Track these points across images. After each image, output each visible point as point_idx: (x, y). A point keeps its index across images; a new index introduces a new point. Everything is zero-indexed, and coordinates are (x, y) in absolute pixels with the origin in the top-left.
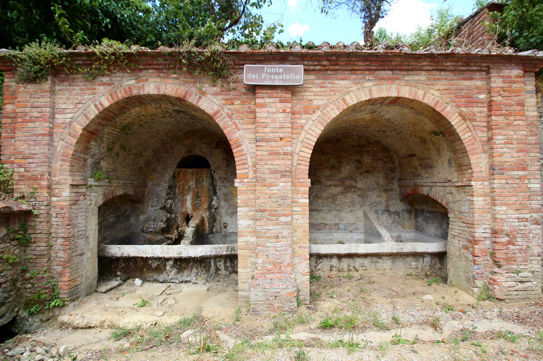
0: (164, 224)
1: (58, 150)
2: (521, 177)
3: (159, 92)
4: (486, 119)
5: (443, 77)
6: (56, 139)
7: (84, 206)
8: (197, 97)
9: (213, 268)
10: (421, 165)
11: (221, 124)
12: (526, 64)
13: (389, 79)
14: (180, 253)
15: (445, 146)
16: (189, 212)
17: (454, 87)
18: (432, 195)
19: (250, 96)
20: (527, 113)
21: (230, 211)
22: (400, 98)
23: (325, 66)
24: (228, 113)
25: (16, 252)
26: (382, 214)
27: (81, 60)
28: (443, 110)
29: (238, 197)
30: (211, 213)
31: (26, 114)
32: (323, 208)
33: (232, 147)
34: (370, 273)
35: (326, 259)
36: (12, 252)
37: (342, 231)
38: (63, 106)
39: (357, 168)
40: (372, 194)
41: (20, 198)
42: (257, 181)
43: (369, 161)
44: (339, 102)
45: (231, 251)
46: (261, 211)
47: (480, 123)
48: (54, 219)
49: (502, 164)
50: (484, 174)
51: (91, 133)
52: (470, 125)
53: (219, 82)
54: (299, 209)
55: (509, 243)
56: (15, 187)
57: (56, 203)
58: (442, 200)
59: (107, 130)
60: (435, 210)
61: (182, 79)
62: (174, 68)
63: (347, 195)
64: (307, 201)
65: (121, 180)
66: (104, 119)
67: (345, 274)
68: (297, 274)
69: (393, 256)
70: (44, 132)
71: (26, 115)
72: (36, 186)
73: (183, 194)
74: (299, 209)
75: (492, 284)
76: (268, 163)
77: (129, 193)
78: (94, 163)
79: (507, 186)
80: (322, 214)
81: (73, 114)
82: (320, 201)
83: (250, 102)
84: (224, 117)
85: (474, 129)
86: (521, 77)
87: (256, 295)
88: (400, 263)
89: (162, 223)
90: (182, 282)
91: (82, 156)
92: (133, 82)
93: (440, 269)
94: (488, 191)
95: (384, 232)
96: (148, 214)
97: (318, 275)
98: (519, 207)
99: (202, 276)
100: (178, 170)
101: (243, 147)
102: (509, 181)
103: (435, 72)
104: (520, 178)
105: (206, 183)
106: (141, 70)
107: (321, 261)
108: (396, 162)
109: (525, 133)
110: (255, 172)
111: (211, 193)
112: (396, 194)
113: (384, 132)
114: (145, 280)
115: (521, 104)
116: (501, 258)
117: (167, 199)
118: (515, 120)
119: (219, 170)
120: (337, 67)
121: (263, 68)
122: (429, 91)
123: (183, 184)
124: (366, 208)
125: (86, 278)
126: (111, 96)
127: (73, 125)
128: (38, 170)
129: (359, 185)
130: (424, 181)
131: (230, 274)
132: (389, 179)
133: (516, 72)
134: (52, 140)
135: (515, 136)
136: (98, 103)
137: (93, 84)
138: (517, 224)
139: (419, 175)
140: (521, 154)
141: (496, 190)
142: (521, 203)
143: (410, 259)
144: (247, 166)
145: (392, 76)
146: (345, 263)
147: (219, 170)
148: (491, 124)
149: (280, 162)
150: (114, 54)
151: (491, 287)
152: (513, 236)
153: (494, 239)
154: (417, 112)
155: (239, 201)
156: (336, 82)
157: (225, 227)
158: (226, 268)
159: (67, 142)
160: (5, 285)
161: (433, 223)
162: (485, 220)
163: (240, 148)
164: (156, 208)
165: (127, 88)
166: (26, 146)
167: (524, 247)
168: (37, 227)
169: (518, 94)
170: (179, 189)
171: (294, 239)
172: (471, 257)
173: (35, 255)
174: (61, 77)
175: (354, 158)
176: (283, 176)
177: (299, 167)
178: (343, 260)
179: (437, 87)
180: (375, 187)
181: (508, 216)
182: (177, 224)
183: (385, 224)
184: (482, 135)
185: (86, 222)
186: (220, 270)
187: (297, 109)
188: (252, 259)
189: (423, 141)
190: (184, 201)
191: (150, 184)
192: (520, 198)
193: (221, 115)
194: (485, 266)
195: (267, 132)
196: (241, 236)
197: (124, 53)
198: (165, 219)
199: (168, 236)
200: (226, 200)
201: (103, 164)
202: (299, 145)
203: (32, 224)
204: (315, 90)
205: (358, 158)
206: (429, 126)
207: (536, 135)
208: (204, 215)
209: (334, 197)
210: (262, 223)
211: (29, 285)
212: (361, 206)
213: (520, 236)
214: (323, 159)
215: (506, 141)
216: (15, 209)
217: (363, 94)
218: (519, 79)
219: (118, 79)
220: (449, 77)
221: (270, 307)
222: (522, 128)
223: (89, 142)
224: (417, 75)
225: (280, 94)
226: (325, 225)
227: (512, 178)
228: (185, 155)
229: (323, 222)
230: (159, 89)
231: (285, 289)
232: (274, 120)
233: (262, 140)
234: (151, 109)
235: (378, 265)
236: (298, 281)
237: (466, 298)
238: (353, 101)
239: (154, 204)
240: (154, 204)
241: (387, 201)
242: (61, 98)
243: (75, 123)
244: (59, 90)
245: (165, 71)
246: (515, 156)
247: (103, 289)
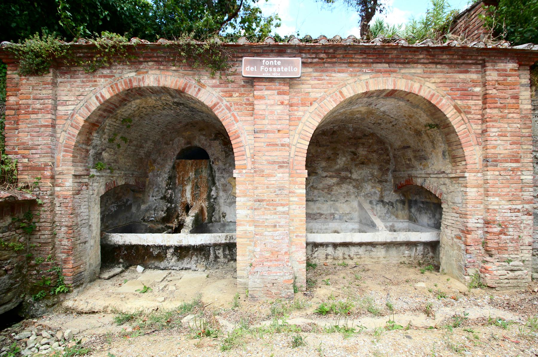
0: (165, 213)
1: (61, 141)
2: (514, 169)
3: (159, 84)
4: (481, 112)
5: (439, 70)
6: (59, 131)
7: (87, 196)
8: (197, 89)
9: (212, 256)
10: (415, 157)
11: (220, 116)
13: (386, 71)
15: (440, 139)
16: (189, 202)
18: (426, 186)
19: (248, 88)
20: (521, 106)
21: (228, 201)
22: (396, 90)
23: (323, 59)
24: (226, 105)
25: (22, 239)
26: (377, 204)
27: (82, 53)
28: (438, 103)
29: (237, 187)
31: (28, 106)
32: (319, 199)
33: (231, 139)
34: (364, 261)
35: (321, 248)
36: (19, 239)
37: (338, 221)
38: (65, 98)
40: (366, 185)
41: (24, 188)
42: (255, 172)
43: (364, 153)
44: (336, 94)
45: (230, 240)
46: (259, 201)
47: (474, 116)
48: (57, 208)
49: (496, 156)
50: (478, 166)
51: (93, 125)
52: (465, 118)
53: (218, 74)
54: (296, 199)
55: (501, 233)
56: (19, 177)
57: (59, 193)
58: (436, 191)
59: (108, 122)
60: (428, 200)
61: (181, 71)
62: (174, 60)
63: (342, 186)
64: (304, 191)
65: (123, 170)
66: (105, 111)
67: (341, 262)
68: (294, 262)
70: (46, 124)
71: (29, 107)
72: (39, 176)
75: (484, 273)
76: (266, 154)
77: (130, 183)
78: (96, 154)
79: (500, 178)
80: (318, 205)
81: (75, 106)
82: (316, 192)
83: (248, 94)
84: (223, 110)
85: (469, 122)
86: (515, 70)
87: (255, 282)
88: (393, 252)
89: (163, 213)
90: (182, 269)
91: (84, 146)
92: (133, 74)
93: (433, 257)
94: (481, 182)
95: (378, 222)
96: (149, 203)
97: (314, 263)
98: (512, 198)
99: (202, 263)
100: (178, 161)
101: (242, 138)
102: (502, 173)
103: (431, 65)
104: (513, 170)
105: (205, 174)
106: (141, 63)
107: (317, 249)
108: (391, 154)
109: (519, 125)
110: (253, 163)
111: (210, 183)
112: (390, 185)
113: (380, 124)
114: (146, 267)
115: (516, 97)
116: (492, 248)
117: (167, 190)
118: (509, 113)
119: (218, 161)
120: (334, 60)
121: (261, 60)
122: (425, 84)
123: (183, 174)
125: (90, 265)
126: (112, 88)
127: (75, 116)
128: (40, 160)
129: (355, 176)
130: (418, 172)
131: (228, 261)
132: (384, 171)
133: (511, 65)
134: (55, 132)
135: (509, 129)
136: (99, 95)
137: (94, 77)
138: (509, 214)
139: (413, 167)
140: (515, 146)
141: (489, 181)
142: (513, 195)
143: (403, 248)
144: (245, 157)
145: (388, 69)
146: (340, 251)
147: (218, 161)
148: (486, 117)
149: (278, 153)
150: (113, 46)
151: (482, 275)
152: (505, 226)
153: (486, 229)
154: (413, 105)
155: (237, 191)
156: (333, 75)
157: (224, 217)
158: (225, 256)
159: (69, 133)
160: (11, 272)
161: (426, 213)
162: (477, 210)
163: (238, 140)
164: (157, 198)
165: (128, 80)
166: (29, 137)
167: (516, 237)
168: (42, 216)
169: (512, 87)
170: (179, 179)
171: (292, 228)
172: (463, 246)
173: (39, 243)
174: (63, 70)
175: (350, 150)
176: (281, 167)
177: (296, 158)
178: (338, 248)
180: (370, 178)
181: (501, 206)
182: (177, 214)
183: (379, 214)
184: (476, 128)
185: (89, 211)
186: (219, 258)
187: (294, 101)
188: (251, 248)
189: (418, 133)
190: (183, 191)
191: (150, 174)
192: (513, 189)
193: (220, 107)
194: (477, 255)
195: (265, 124)
196: (240, 225)
197: (124, 46)
198: (165, 208)
199: (168, 225)
200: (225, 190)
201: (105, 155)
202: (297, 136)
203: (37, 213)
205: (353, 150)
206: (424, 118)
207: (530, 127)
208: (203, 205)
209: (329, 188)
210: (260, 212)
211: (35, 272)
212: (356, 196)
213: (512, 226)
214: (319, 151)
215: (500, 133)
216: (20, 198)
217: (360, 86)
218: (514, 73)
219: (119, 71)
220: (444, 70)
221: (267, 293)
222: (516, 121)
223: (91, 133)
224: (413, 68)
225: (278, 87)
226: (321, 214)
227: (505, 169)
228: (184, 147)
229: (318, 212)
230: (159, 81)
231: (282, 276)
232: (272, 113)
233: (261, 132)
234: (152, 100)
235: (373, 254)
236: (295, 269)
237: (458, 286)
238: (350, 93)
239: (155, 194)
240: (155, 194)
241: (381, 192)
242: (63, 90)
243: (77, 115)
244: (61, 82)
245: (164, 63)
246: (508, 148)
247: (106, 275)
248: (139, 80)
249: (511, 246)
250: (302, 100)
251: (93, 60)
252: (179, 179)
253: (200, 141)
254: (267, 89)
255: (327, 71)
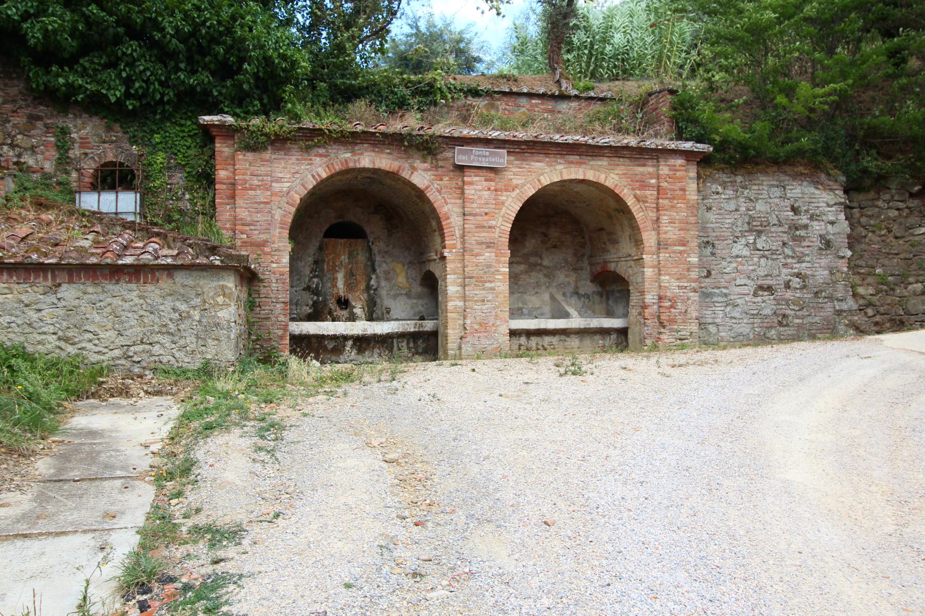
6: (274, 207)
9: (395, 348)
10: (609, 240)
11: (431, 198)
12: (688, 155)
13: (577, 163)
14: (365, 330)
17: (630, 172)
18: (618, 271)
19: (458, 173)
21: (392, 293)
30: (369, 295)
31: (245, 181)
38: (280, 175)
39: (543, 242)
53: (429, 158)
54: (500, 277)
55: (671, 307)
64: (508, 270)
69: (582, 333)
73: (334, 270)
74: (500, 277)
88: (587, 342)
92: (348, 155)
94: (656, 263)
95: (572, 311)
100: (326, 240)
101: (452, 220)
104: (681, 252)
105: (362, 257)
108: (587, 237)
110: (463, 243)
111: (369, 269)
112: (586, 274)
113: (574, 202)
115: (683, 190)
124: (553, 290)
127: (291, 193)
128: (259, 237)
129: (546, 262)
132: (579, 257)
133: (680, 162)
139: (608, 251)
143: (597, 337)
146: (534, 341)
149: (485, 234)
157: (388, 312)
170: (328, 264)
172: (642, 320)
176: (488, 247)
179: (617, 172)
181: (671, 285)
187: (498, 187)
194: (653, 327)
200: (387, 279)
202: (501, 219)
203: (257, 288)
204: (514, 170)
205: (544, 230)
206: (613, 204)
207: (696, 216)
227: (674, 252)
228: (334, 221)
232: (480, 197)
233: (470, 214)
235: (566, 343)
241: (576, 281)
248: (355, 161)
249: (680, 318)
250: (505, 186)
251: (311, 139)
252: (328, 264)
253: (355, 216)
254: (476, 176)
255: (526, 160)
